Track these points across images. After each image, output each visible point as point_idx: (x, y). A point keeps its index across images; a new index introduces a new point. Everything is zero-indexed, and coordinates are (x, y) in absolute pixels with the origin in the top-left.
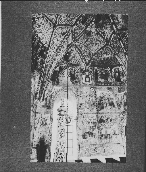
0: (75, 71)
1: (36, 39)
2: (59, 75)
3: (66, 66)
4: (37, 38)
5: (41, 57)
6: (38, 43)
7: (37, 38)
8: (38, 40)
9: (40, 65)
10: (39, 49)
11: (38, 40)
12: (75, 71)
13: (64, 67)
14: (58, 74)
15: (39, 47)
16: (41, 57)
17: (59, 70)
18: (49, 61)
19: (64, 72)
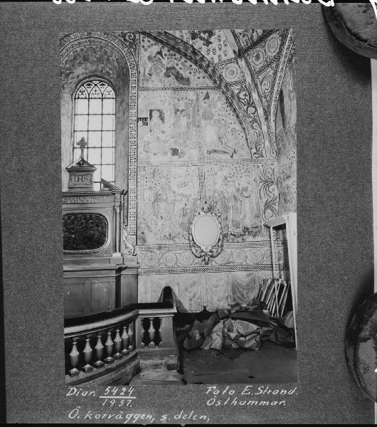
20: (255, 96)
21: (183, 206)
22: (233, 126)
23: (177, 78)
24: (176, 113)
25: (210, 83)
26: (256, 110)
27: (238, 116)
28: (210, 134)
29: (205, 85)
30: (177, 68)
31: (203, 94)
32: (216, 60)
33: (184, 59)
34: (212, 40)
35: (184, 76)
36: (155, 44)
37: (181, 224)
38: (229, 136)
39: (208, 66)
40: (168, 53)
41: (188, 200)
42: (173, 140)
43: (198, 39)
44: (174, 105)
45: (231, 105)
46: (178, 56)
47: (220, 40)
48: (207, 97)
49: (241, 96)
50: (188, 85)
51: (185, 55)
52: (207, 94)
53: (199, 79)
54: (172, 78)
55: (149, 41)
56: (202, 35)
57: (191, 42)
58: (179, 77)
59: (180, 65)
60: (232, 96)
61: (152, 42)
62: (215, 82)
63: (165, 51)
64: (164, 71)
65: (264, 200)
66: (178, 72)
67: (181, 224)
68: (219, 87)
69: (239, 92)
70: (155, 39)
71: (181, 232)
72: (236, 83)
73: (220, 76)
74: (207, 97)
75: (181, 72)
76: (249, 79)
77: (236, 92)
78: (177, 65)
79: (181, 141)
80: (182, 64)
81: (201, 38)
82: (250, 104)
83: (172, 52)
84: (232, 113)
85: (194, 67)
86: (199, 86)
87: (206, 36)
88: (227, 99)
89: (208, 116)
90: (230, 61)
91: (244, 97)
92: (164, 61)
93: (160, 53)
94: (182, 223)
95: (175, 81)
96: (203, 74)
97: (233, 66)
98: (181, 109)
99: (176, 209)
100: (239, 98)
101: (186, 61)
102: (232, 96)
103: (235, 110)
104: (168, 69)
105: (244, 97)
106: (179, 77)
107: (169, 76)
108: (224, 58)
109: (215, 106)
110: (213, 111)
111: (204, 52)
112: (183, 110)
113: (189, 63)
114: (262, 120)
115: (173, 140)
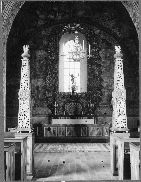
21: (108, 93)
24: (106, 58)
35: (109, 42)
36: (98, 30)
37: (107, 100)
39: (119, 40)
40: (103, 33)
41: (110, 91)
43: (116, 30)
44: (105, 55)
55: (96, 28)
57: (112, 30)
58: (107, 43)
59: (108, 38)
61: (97, 28)
64: (101, 41)
67: (107, 100)
70: (97, 27)
71: (107, 102)
75: (108, 41)
78: (107, 38)
79: (108, 69)
80: (109, 38)
83: (104, 33)
85: (113, 39)
92: (101, 37)
93: (99, 33)
94: (107, 99)
95: (106, 45)
98: (108, 56)
99: (105, 94)
101: (110, 37)
104: (103, 40)
106: (107, 43)
108: (125, 37)
113: (111, 37)
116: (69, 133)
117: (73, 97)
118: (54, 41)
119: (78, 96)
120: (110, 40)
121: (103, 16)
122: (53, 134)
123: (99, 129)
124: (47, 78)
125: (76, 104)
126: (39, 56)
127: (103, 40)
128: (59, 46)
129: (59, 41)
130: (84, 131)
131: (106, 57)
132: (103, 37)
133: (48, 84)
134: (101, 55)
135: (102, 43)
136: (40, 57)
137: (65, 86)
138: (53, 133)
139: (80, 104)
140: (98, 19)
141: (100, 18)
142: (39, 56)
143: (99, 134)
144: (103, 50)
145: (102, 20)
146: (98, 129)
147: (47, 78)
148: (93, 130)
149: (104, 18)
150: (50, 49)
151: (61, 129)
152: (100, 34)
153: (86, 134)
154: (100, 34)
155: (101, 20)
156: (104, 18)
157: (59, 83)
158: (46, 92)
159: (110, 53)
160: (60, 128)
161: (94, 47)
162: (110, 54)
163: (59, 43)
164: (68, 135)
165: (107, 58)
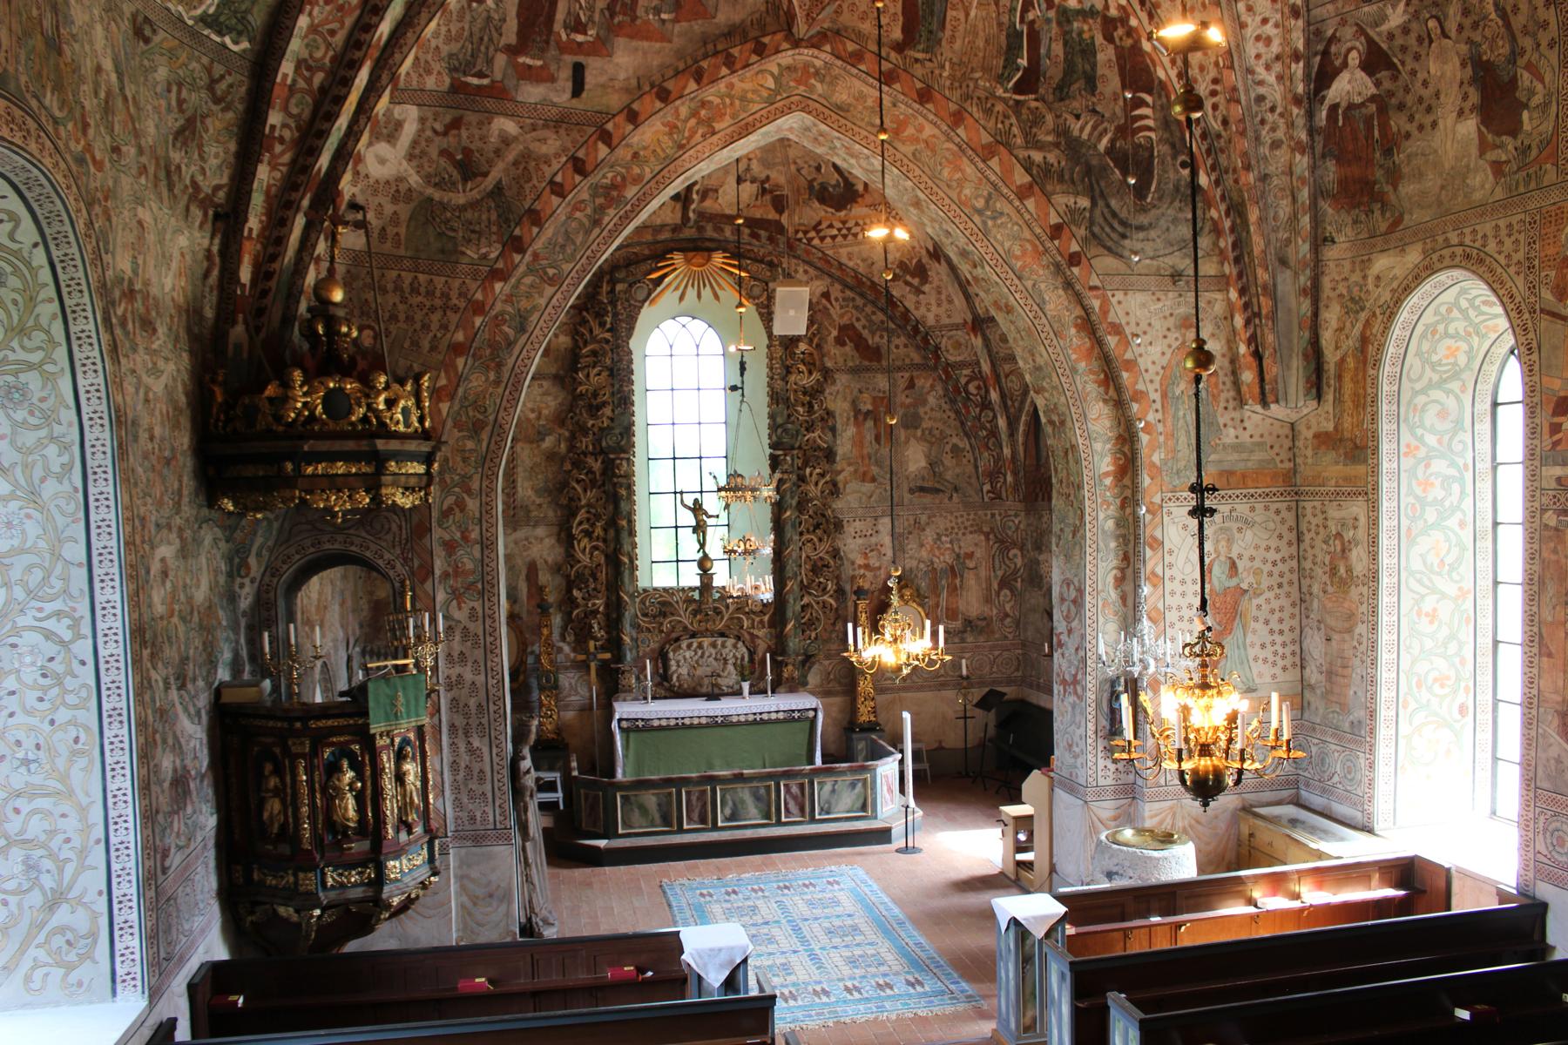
0: (1508, 25)
1: (1033, 22)
2: (1398, 122)
3: (1416, 15)
4: (1031, 16)
5: (1149, 99)
6: (1066, 36)
7: (1031, 16)
8: (1052, 14)
9: (1174, 157)
10: (1101, 57)
11: (1052, 14)
12: (1508, 25)
13: (1405, 30)
14: (1384, 127)
15: (1089, 51)
16: (1149, 99)
17: (1378, 84)
18: (1214, 93)
19: (1425, 84)
20: (994, 396)
22: (955, 440)
23: (857, 348)
24: (856, 418)
25: (916, 358)
26: (995, 417)
27: (962, 424)
28: (915, 459)
29: (907, 361)
30: (858, 326)
31: (902, 379)
32: (931, 320)
33: (869, 309)
34: (926, 288)
36: (817, 277)
38: (948, 461)
40: (840, 295)
42: (852, 469)
45: (953, 402)
46: (860, 301)
47: (939, 293)
48: (911, 385)
49: (972, 388)
50: (879, 361)
51: (873, 303)
52: (912, 379)
53: (900, 349)
54: (849, 348)
56: (908, 278)
58: (861, 345)
59: (863, 321)
60: (957, 390)
61: (811, 271)
62: (925, 358)
63: (836, 291)
64: (835, 333)
65: (1000, 573)
66: (860, 336)
68: (935, 368)
69: (967, 383)
72: (962, 365)
73: (937, 348)
74: (911, 385)
75: (865, 333)
76: (986, 367)
77: (963, 381)
81: (907, 283)
82: (986, 405)
83: (849, 293)
84: (953, 416)
86: (899, 363)
87: (916, 281)
88: (946, 390)
89: (912, 422)
90: (956, 327)
91: (974, 391)
93: (826, 295)
96: (901, 341)
97: (960, 335)
100: (967, 392)
102: (957, 390)
103: (957, 412)
104: (842, 329)
105: (974, 391)
106: (861, 345)
107: (843, 344)
108: (946, 321)
109: (925, 402)
110: (921, 411)
111: (910, 305)
112: (869, 412)
113: (880, 316)
114: (1004, 437)
115: (852, 469)
116: (728, 812)
117: (704, 607)
118: (607, 335)
119: (727, 607)
120: (873, 333)
121: (844, 223)
122: (658, 820)
123: (860, 785)
124: (580, 523)
125: (723, 646)
126: (533, 411)
127: (842, 329)
128: (631, 361)
129: (629, 336)
130: (795, 798)
131: (857, 412)
132: (842, 316)
133: (583, 551)
134: (831, 406)
135: (840, 342)
136: (539, 418)
137: (664, 559)
138: (657, 817)
139: (740, 644)
140: (818, 232)
141: (831, 226)
142: (533, 411)
143: (859, 804)
144: (842, 380)
145: (839, 239)
146: (853, 785)
147: (580, 523)
148: (833, 791)
149: (849, 229)
150: (588, 376)
151: (694, 798)
152: (829, 301)
153: (802, 810)
154: (829, 301)
155: (834, 237)
156: (849, 229)
157: (634, 545)
158: (575, 593)
159: (876, 394)
160: (688, 793)
161: (802, 367)
162: (874, 398)
163: (633, 344)
164: (727, 819)
165: (861, 418)
